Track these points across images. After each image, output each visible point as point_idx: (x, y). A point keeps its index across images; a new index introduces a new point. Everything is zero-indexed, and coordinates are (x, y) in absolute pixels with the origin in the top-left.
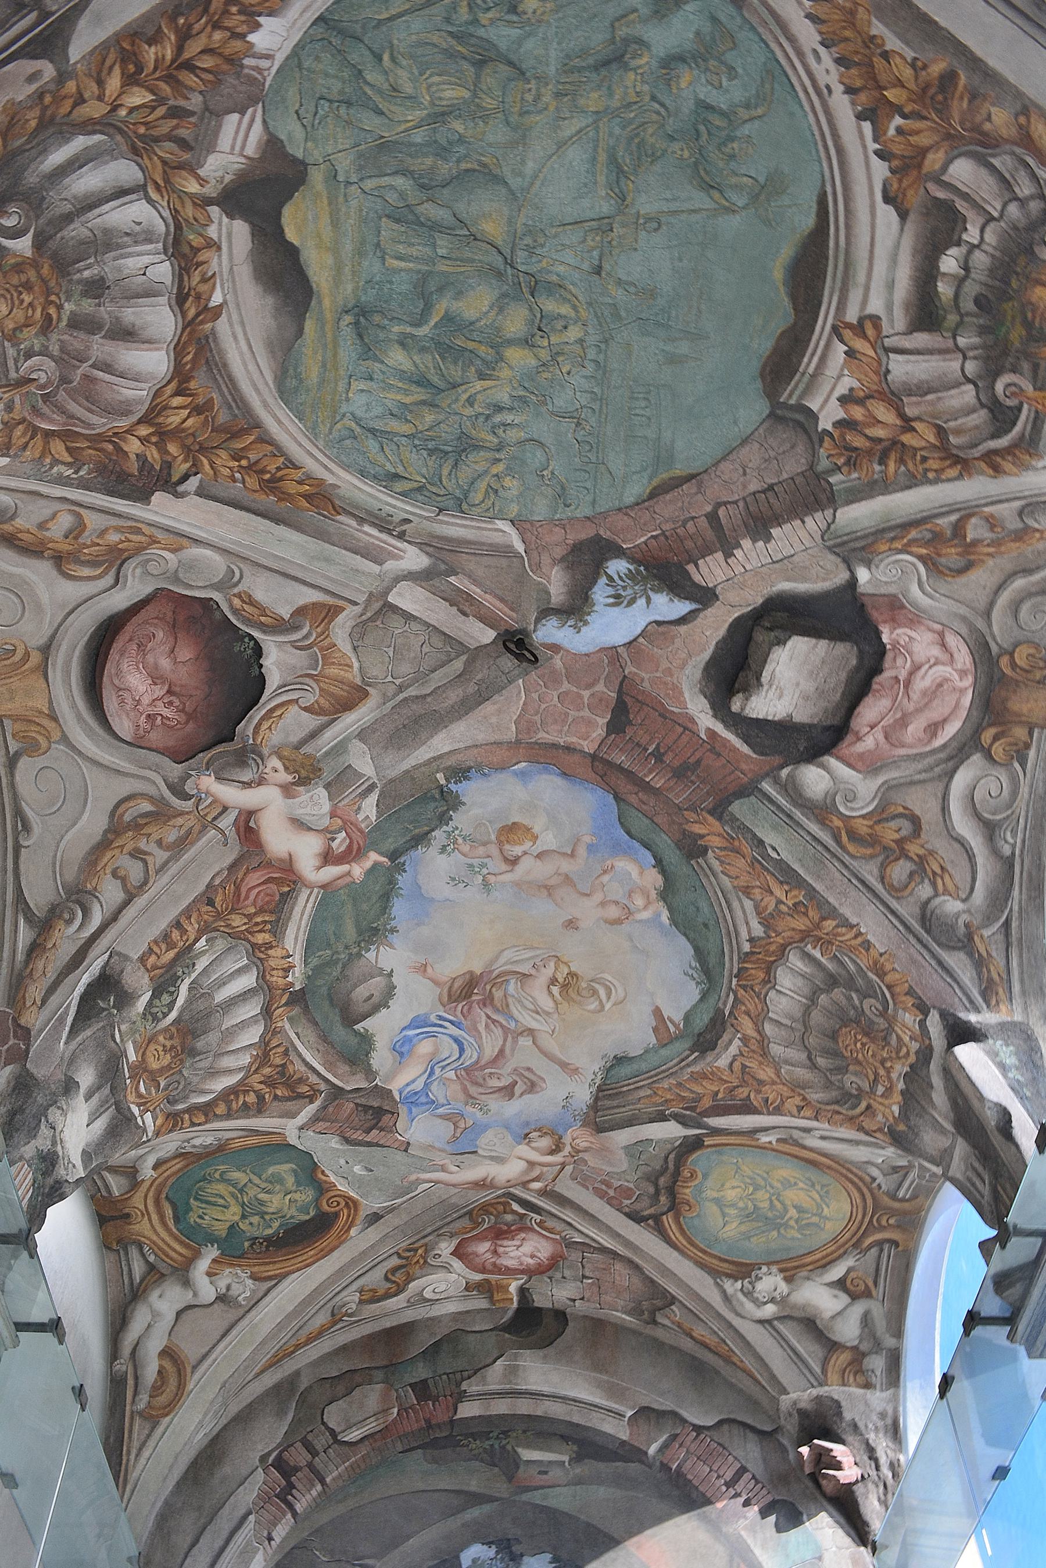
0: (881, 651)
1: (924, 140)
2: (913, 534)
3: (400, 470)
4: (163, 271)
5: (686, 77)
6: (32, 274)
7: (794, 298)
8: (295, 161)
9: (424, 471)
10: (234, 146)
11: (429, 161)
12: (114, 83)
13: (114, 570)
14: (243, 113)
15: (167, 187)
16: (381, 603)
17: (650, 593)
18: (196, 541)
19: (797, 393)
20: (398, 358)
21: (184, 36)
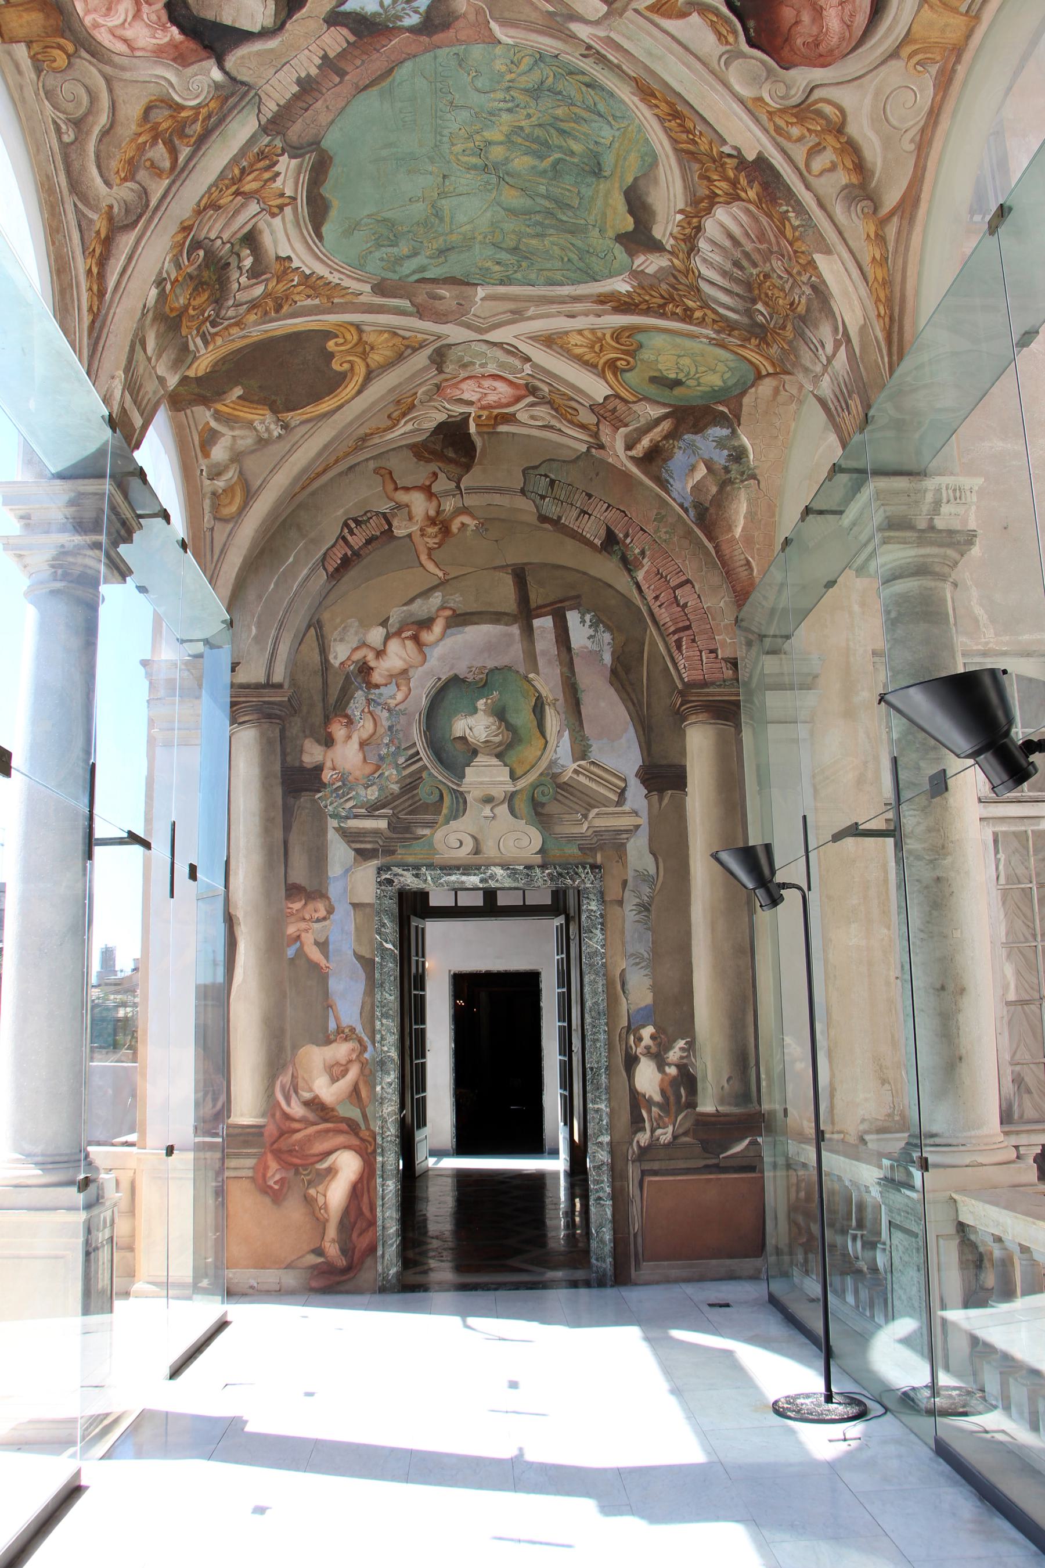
0: (173, 20)
1: (280, 285)
2: (198, 127)
3: (584, 88)
4: (702, 244)
5: (406, 251)
6: (763, 296)
7: (323, 198)
8: (621, 244)
9: (566, 83)
10: (652, 264)
11: (547, 222)
12: (698, 314)
13: (810, 100)
14: (642, 271)
15: (687, 271)
16: (615, 6)
17: (381, 11)
18: (741, 101)
19: (305, 165)
20: (576, 147)
21: (663, 306)
